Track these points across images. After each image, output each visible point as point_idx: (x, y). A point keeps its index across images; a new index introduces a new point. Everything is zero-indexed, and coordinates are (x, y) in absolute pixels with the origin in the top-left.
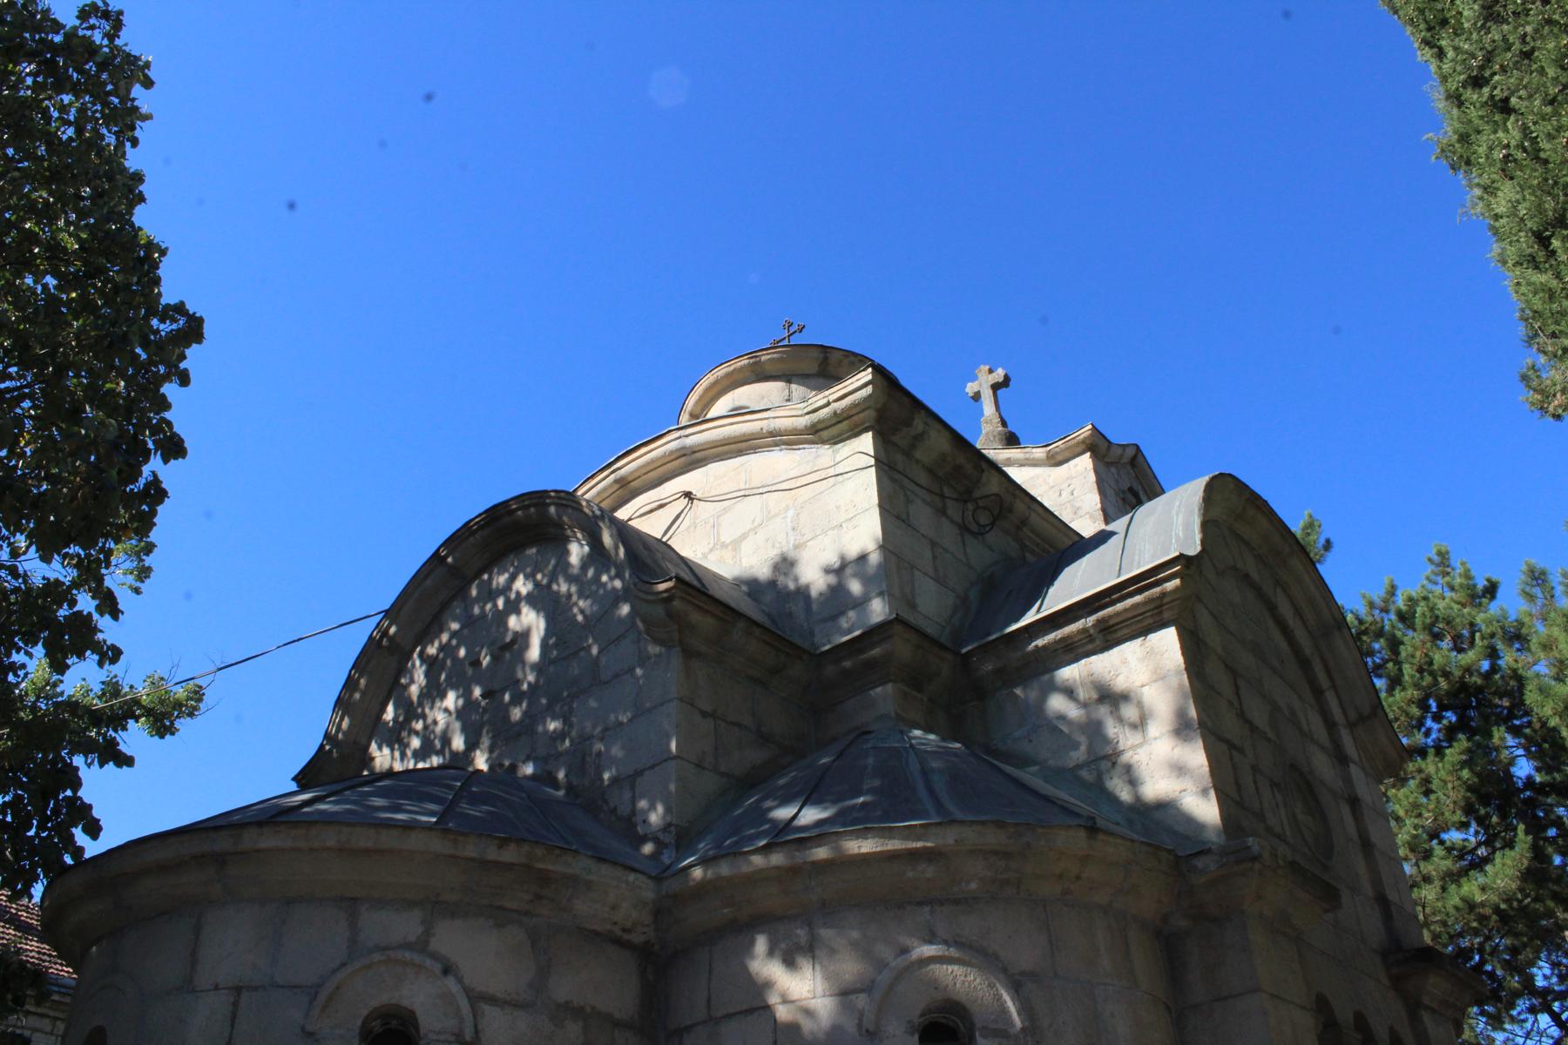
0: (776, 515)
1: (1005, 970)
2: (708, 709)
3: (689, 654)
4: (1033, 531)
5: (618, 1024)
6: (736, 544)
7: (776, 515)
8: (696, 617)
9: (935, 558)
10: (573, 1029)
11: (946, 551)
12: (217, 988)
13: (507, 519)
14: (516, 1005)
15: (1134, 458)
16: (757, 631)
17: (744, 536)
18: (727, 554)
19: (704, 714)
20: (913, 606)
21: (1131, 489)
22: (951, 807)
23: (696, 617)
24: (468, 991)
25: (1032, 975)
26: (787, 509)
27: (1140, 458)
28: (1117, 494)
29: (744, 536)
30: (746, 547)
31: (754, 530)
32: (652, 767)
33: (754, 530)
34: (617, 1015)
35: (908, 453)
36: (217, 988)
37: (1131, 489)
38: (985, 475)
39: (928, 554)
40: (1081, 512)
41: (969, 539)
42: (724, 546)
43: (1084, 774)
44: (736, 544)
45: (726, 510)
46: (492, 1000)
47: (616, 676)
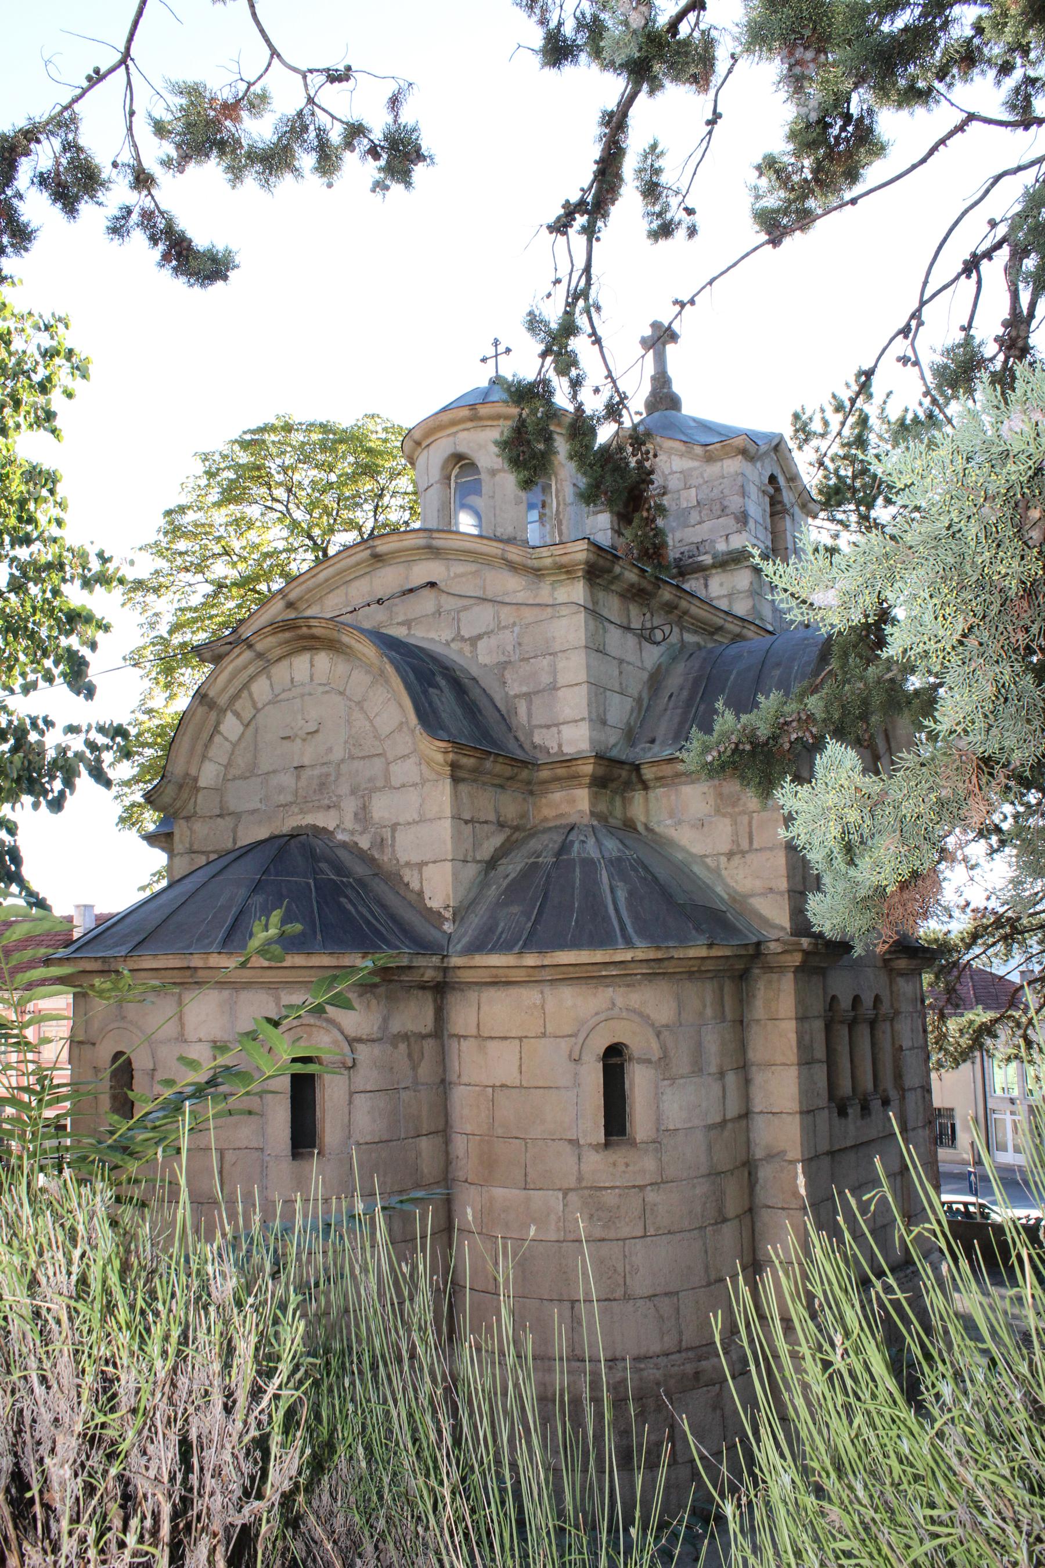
0: (505, 627)
1: (653, 1025)
2: (467, 817)
3: (456, 780)
4: (692, 617)
5: (424, 1037)
6: (474, 641)
7: (505, 627)
8: (464, 761)
9: (621, 673)
10: (403, 1047)
11: (629, 663)
12: (200, 1041)
13: (305, 630)
14: (373, 1041)
15: (777, 445)
16: (501, 759)
17: (480, 637)
18: (467, 648)
19: (466, 822)
20: (604, 723)
21: (773, 479)
22: (630, 929)
23: (464, 761)
24: (346, 1038)
25: (667, 1026)
26: (514, 624)
27: (783, 445)
28: (759, 489)
29: (480, 637)
30: (481, 645)
31: (488, 633)
32: (435, 862)
33: (488, 633)
34: (424, 1032)
35: (606, 589)
36: (200, 1041)
37: (773, 479)
38: (660, 592)
39: (616, 673)
40: (728, 511)
41: (645, 644)
42: (463, 639)
43: (708, 860)
44: (474, 641)
45: (465, 608)
46: (359, 1040)
47: (404, 786)
